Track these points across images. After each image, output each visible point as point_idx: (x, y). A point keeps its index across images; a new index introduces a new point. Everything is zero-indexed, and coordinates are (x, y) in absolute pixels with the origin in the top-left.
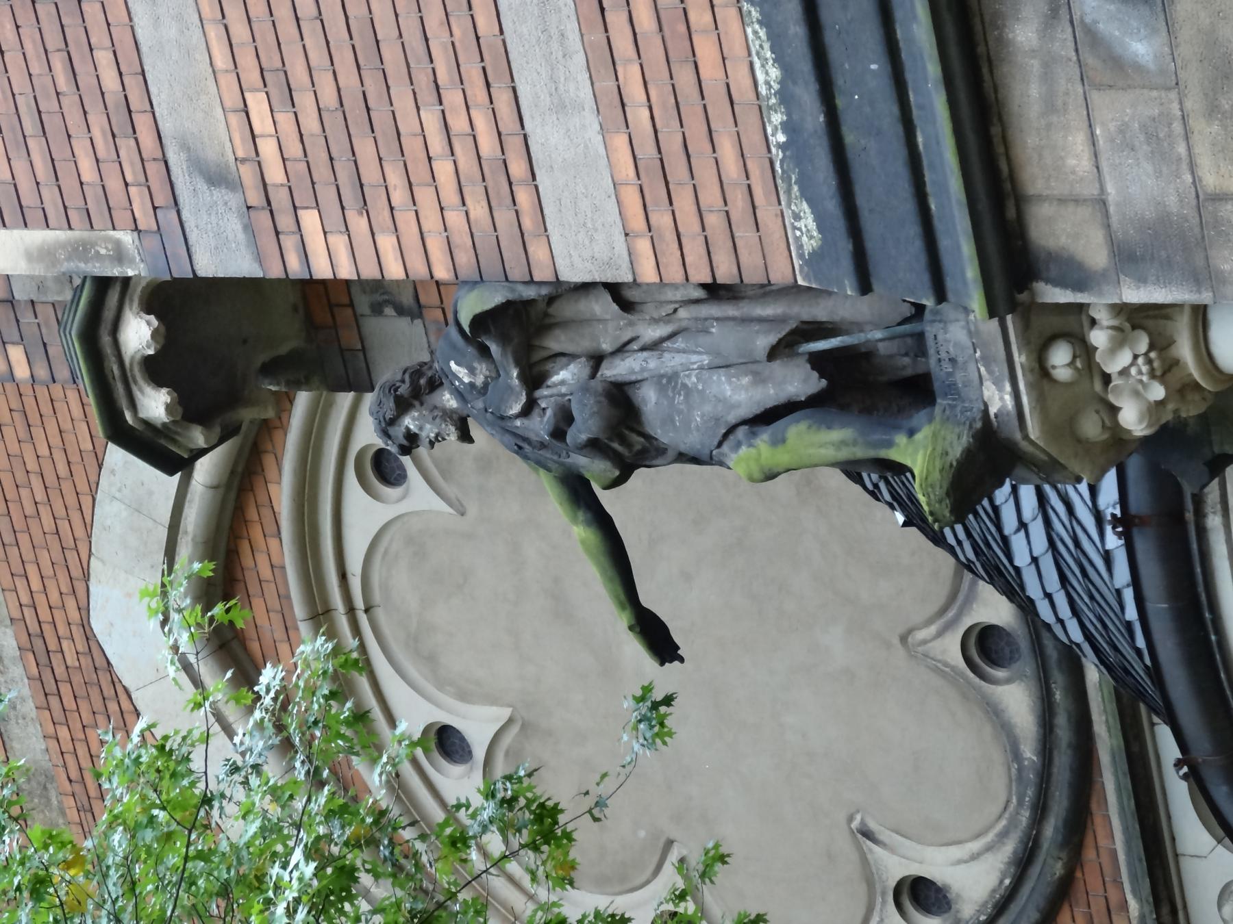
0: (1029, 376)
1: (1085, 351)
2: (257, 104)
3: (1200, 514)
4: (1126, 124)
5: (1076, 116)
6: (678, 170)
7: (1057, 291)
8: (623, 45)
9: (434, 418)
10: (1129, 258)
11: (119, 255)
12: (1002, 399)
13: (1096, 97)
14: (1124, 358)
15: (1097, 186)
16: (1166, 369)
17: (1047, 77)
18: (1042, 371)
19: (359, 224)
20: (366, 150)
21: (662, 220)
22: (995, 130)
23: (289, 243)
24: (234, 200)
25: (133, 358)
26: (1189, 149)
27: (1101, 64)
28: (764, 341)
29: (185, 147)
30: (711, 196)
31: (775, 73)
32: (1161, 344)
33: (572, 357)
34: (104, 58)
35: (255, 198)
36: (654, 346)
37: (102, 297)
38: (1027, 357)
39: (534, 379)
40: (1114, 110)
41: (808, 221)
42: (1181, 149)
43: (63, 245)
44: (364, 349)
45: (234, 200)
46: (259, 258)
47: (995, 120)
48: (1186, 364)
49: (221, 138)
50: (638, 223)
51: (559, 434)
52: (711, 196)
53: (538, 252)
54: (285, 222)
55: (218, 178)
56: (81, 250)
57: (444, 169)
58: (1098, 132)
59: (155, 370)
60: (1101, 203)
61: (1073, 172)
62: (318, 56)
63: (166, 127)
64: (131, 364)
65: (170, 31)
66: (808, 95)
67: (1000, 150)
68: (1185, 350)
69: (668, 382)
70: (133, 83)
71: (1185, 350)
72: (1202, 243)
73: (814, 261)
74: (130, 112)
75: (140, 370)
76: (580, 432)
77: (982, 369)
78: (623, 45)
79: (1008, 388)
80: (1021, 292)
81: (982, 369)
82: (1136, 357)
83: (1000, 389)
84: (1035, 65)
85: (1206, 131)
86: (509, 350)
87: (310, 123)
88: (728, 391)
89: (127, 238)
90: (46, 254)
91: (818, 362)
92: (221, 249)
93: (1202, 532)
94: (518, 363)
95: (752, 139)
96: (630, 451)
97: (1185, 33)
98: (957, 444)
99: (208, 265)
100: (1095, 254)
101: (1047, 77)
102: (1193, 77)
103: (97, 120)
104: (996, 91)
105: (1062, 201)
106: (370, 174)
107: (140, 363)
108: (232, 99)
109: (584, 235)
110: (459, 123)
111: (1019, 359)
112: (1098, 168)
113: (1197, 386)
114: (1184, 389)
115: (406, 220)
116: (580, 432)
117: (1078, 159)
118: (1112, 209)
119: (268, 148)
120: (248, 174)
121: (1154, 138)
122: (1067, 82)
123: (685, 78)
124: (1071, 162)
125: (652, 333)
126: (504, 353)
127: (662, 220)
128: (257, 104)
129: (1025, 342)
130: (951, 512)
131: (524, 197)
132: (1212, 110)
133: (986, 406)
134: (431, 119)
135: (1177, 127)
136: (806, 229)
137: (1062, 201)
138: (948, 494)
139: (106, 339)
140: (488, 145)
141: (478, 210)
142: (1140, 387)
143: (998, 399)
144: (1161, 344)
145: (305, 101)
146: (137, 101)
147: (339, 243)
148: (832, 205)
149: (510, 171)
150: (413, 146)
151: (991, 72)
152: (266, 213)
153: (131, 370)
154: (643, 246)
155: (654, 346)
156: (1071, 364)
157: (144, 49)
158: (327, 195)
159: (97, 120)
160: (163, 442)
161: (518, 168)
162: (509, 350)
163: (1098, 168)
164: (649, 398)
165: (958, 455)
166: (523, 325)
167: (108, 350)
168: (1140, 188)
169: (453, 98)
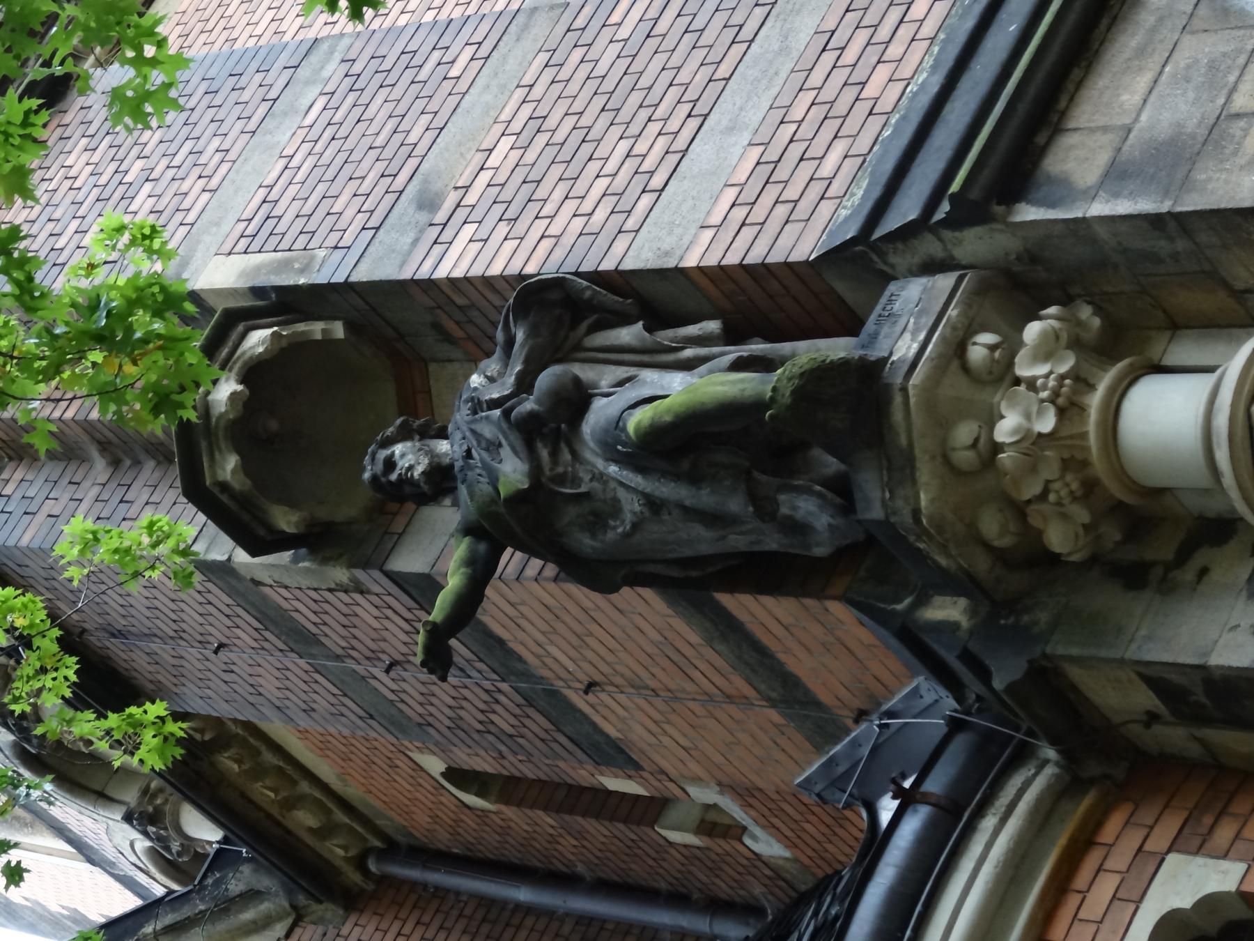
0: (948, 330)
3: (979, 813)
4: (1197, 61)
7: (1033, 209)
9: (420, 450)
12: (909, 347)
14: (1041, 370)
15: (1134, 115)
22: (1076, 73)
25: (244, 353)
26: (1236, 83)
38: (958, 316)
42: (1232, 78)
43: (271, 263)
44: (400, 535)
47: (1084, 64)
48: (1089, 416)
56: (285, 265)
58: (1167, 69)
59: (253, 373)
61: (1121, 106)
64: (239, 358)
67: (1071, 87)
68: (1095, 400)
75: (241, 368)
77: (912, 320)
79: (922, 336)
80: (999, 204)
81: (912, 320)
82: (1051, 372)
83: (913, 340)
86: (530, 342)
88: (664, 489)
93: (970, 829)
94: (527, 362)
96: (551, 470)
104: (1102, 43)
105: (1092, 130)
107: (246, 363)
111: (952, 312)
112: (1145, 101)
113: (1085, 463)
118: (1131, 136)
120: (452, 198)
124: (1125, 97)
126: (523, 345)
129: (967, 304)
130: (793, 392)
133: (891, 354)
135: (1242, 60)
137: (1092, 130)
138: (802, 374)
139: (241, 328)
142: (1035, 408)
146: (420, 150)
151: (1109, 29)
153: (235, 363)
156: (992, 348)
157: (459, 110)
160: (204, 444)
162: (530, 342)
163: (1145, 101)
165: (836, 358)
167: (234, 336)
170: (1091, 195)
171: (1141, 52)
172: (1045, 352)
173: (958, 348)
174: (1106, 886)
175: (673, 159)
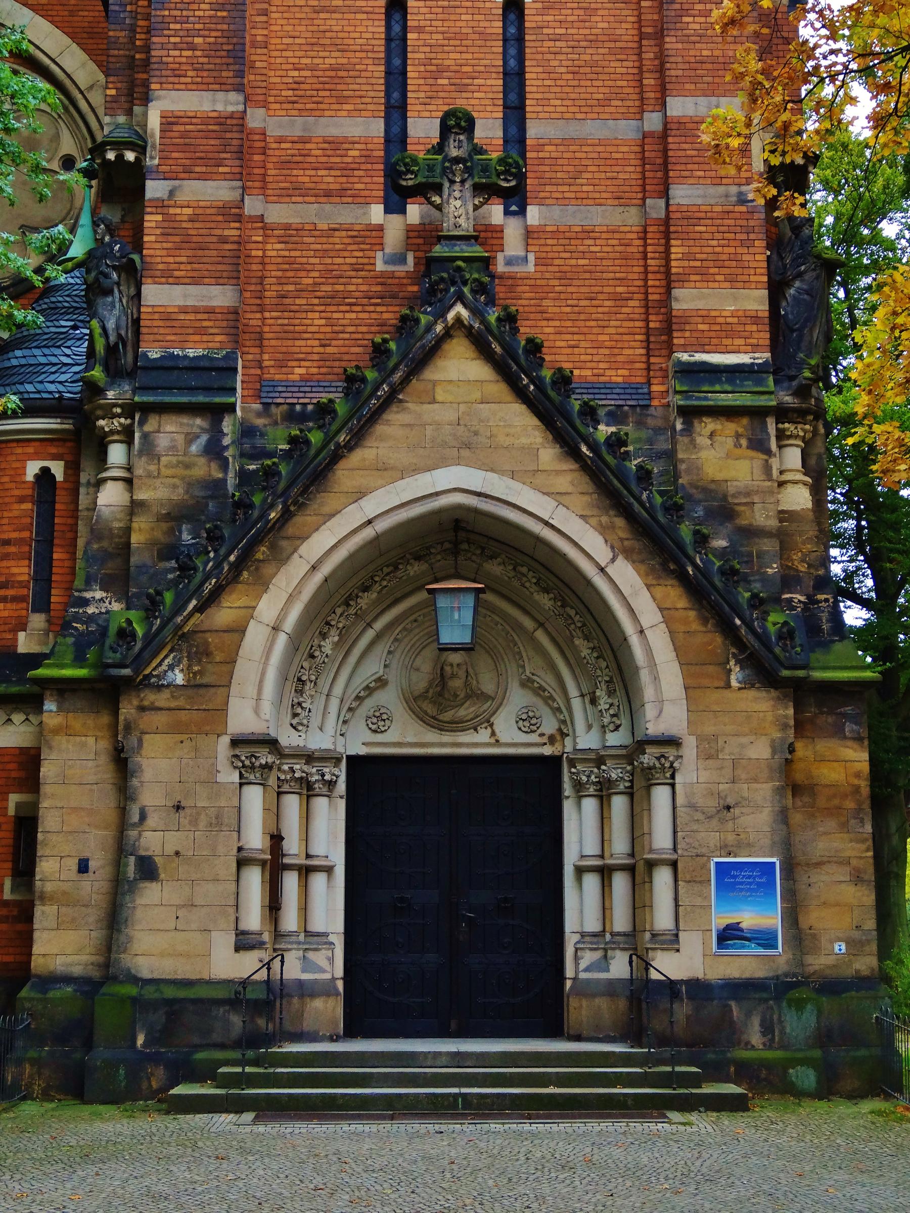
1: (119, 416)
2: (189, 211)
5: (178, 430)
6: (169, 323)
8: (200, 316)
10: (145, 436)
11: (152, 158)
13: (183, 436)
16: (112, 432)
17: (188, 425)
18: (115, 405)
19: (158, 232)
20: (177, 239)
21: (156, 316)
23: (154, 210)
24: (165, 197)
27: (190, 439)
28: (123, 333)
29: (180, 186)
30: (162, 331)
31: (191, 355)
32: (118, 432)
33: (119, 277)
34: (204, 169)
35: (166, 203)
36: (121, 300)
37: (141, 149)
39: (114, 268)
40: (180, 439)
41: (155, 356)
45: (165, 197)
46: (150, 200)
49: (181, 197)
50: (156, 310)
51: (102, 273)
52: (162, 331)
53: (149, 280)
54: (159, 210)
55: (171, 193)
57: (171, 260)
60: (159, 432)
62: (202, 232)
63: (185, 182)
65: (209, 191)
66: (186, 363)
68: (116, 437)
69: (113, 305)
70: (196, 175)
71: (116, 437)
72: (148, 454)
73: (145, 355)
74: (188, 173)
76: (102, 279)
78: (200, 316)
84: (191, 422)
85: (174, 460)
87: (184, 225)
89: (156, 162)
90: (153, 135)
91: (116, 344)
92: (154, 189)
93: (56, 417)
95: (176, 344)
97: (197, 459)
98: (101, 384)
99: (149, 184)
100: (147, 428)
101: (188, 425)
102: (186, 459)
103: (188, 162)
106: (171, 238)
108: (191, 204)
109: (155, 295)
110: (182, 267)
114: (107, 434)
115: (158, 246)
116: (102, 279)
117: (169, 428)
119: (178, 211)
120: (172, 203)
121: (173, 448)
122: (186, 430)
123: (191, 331)
125: (124, 301)
127: (156, 316)
128: (189, 211)
131: (163, 280)
132: (179, 462)
134: (184, 259)
136: (154, 355)
140: (177, 273)
141: (160, 267)
143: (110, 394)
144: (118, 432)
145: (190, 225)
147: (153, 224)
148: (159, 364)
149: (169, 277)
150: (177, 252)
152: (160, 205)
154: (150, 310)
155: (121, 300)
158: (166, 225)
159: (188, 162)
161: (171, 280)
164: (110, 299)
166: (133, 274)
168: (162, 442)
169: (189, 267)
170: (141, 430)
171: (181, 424)
172: (120, 424)
173: (115, 405)
174: (53, 450)
175: (177, 281)
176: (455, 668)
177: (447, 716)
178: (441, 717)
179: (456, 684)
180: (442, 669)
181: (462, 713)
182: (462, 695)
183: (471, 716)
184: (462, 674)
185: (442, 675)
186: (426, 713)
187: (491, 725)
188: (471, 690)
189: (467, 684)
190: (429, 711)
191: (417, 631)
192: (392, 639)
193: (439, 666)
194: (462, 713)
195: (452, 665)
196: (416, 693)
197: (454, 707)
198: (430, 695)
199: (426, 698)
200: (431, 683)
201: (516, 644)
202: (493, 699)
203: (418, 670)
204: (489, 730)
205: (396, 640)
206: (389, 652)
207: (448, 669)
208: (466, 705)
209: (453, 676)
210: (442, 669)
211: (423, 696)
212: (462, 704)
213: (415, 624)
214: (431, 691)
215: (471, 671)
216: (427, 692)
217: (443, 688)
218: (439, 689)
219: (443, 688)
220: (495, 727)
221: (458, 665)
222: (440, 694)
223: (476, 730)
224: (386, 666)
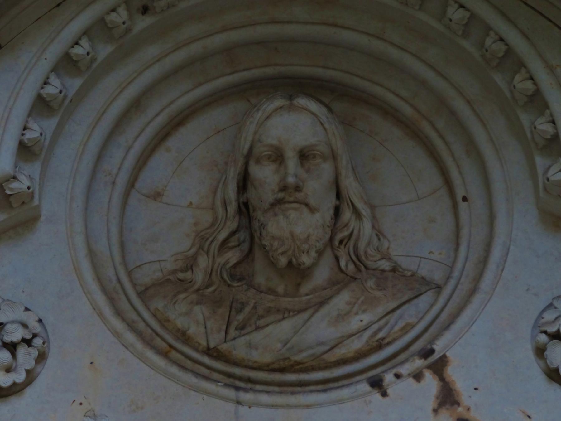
176: (292, 163)
177: (269, 340)
178: (239, 348)
179: (299, 227)
180: (244, 182)
181: (319, 330)
182: (322, 274)
183: (357, 344)
184: (317, 187)
185: (245, 209)
186: (183, 336)
187: (439, 367)
188: (358, 261)
189: (336, 239)
190: (195, 331)
191: (152, 51)
192: (54, 51)
193: (233, 174)
194: (319, 330)
195: (278, 156)
196: (146, 276)
197: (285, 313)
198: (199, 277)
199: (183, 285)
200: (202, 240)
201: (521, 65)
202: (439, 288)
203: (157, 196)
204: (431, 383)
205: (67, 64)
206: (42, 105)
207: (265, 174)
208: (341, 300)
209: (289, 195)
210: (244, 182)
211: (174, 283)
212: (322, 304)
213: (143, 23)
214: (203, 262)
215: (350, 184)
216: (190, 264)
217: (249, 255)
218: (232, 257)
219: (249, 255)
220: (451, 372)
221: (304, 156)
222: (239, 274)
223: (377, 384)
224: (25, 151)
